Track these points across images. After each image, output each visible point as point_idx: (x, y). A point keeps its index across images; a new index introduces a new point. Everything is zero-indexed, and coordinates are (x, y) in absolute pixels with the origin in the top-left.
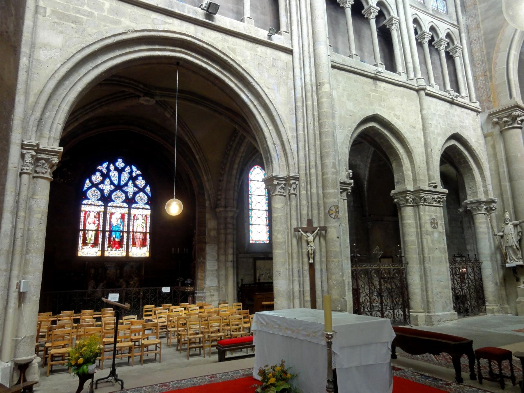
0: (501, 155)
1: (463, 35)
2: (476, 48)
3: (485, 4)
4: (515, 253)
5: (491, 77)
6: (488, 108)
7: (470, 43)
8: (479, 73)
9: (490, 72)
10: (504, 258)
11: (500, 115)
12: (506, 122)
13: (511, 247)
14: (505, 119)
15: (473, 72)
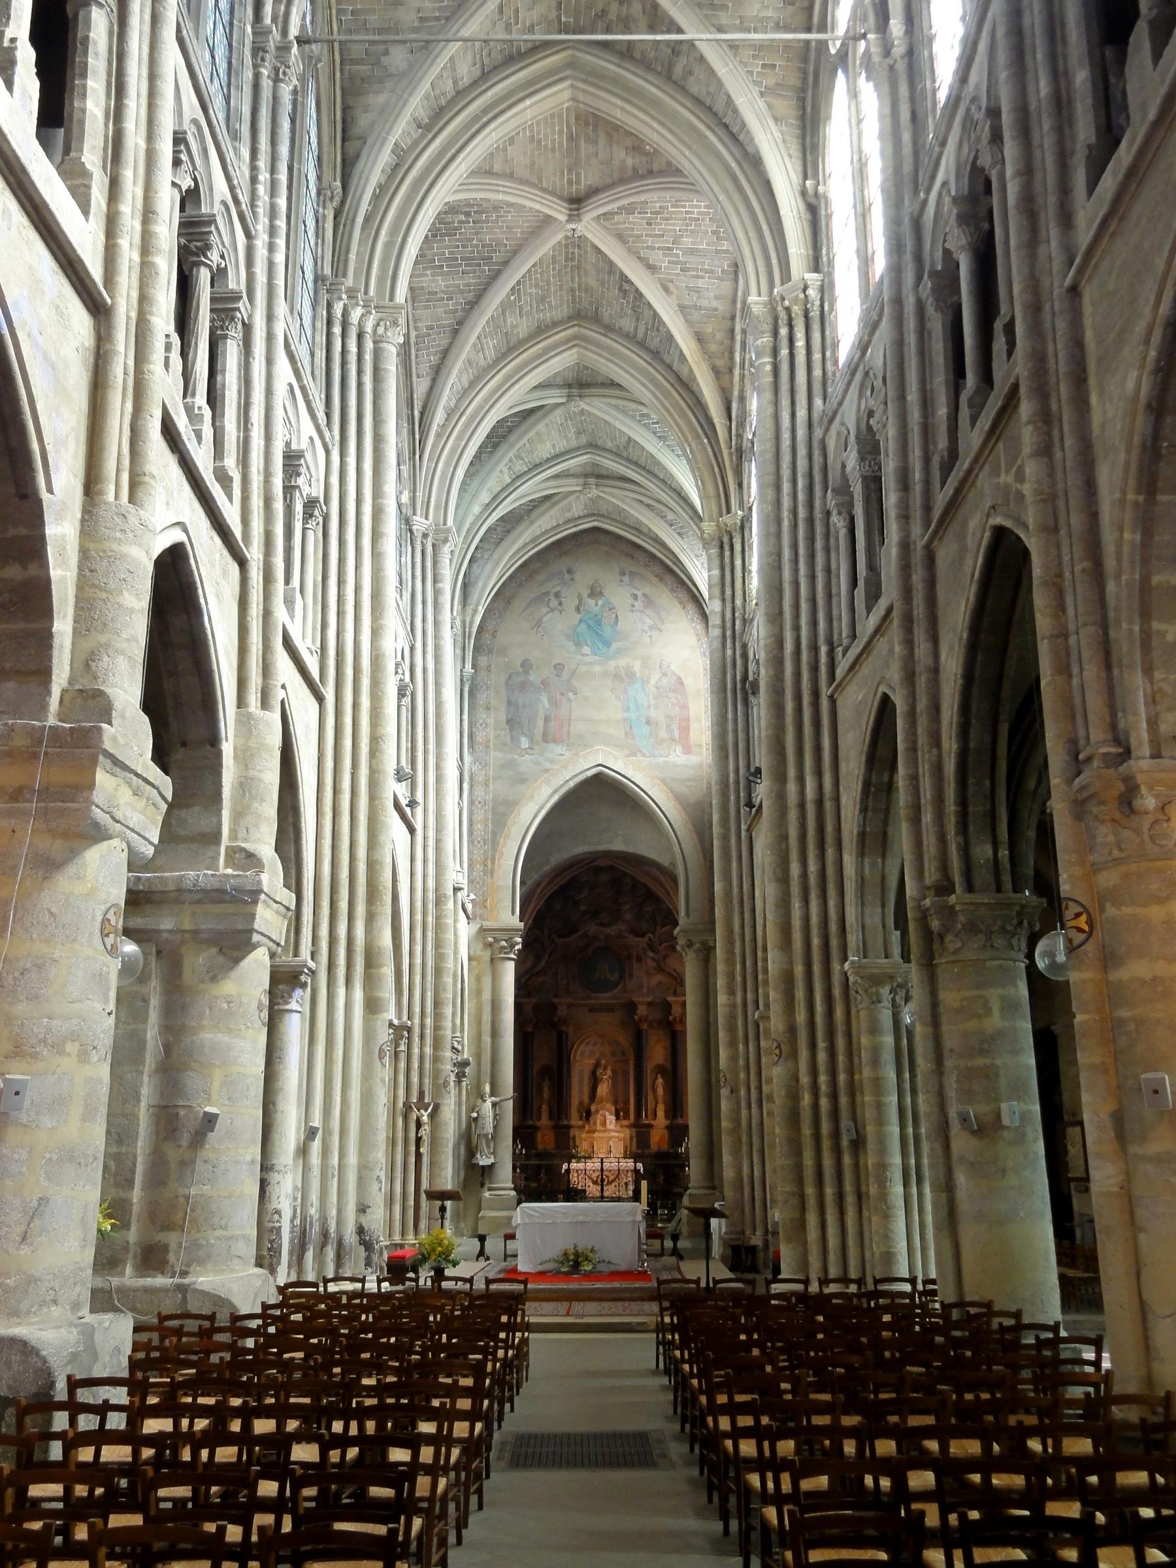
0: (487, 995)
1: (466, 786)
2: (479, 816)
3: (500, 755)
4: (488, 1146)
5: (492, 872)
6: (482, 918)
7: (471, 802)
8: (477, 857)
9: (493, 863)
10: (471, 1152)
11: (498, 935)
12: (503, 948)
13: (486, 1136)
14: (504, 943)
15: (470, 852)
